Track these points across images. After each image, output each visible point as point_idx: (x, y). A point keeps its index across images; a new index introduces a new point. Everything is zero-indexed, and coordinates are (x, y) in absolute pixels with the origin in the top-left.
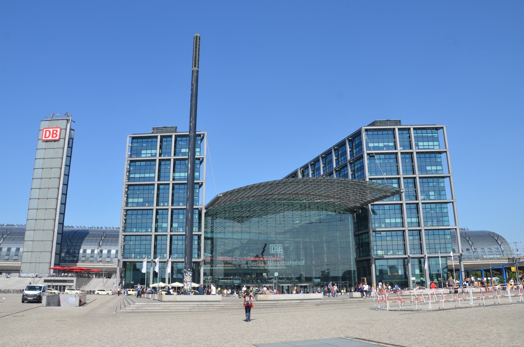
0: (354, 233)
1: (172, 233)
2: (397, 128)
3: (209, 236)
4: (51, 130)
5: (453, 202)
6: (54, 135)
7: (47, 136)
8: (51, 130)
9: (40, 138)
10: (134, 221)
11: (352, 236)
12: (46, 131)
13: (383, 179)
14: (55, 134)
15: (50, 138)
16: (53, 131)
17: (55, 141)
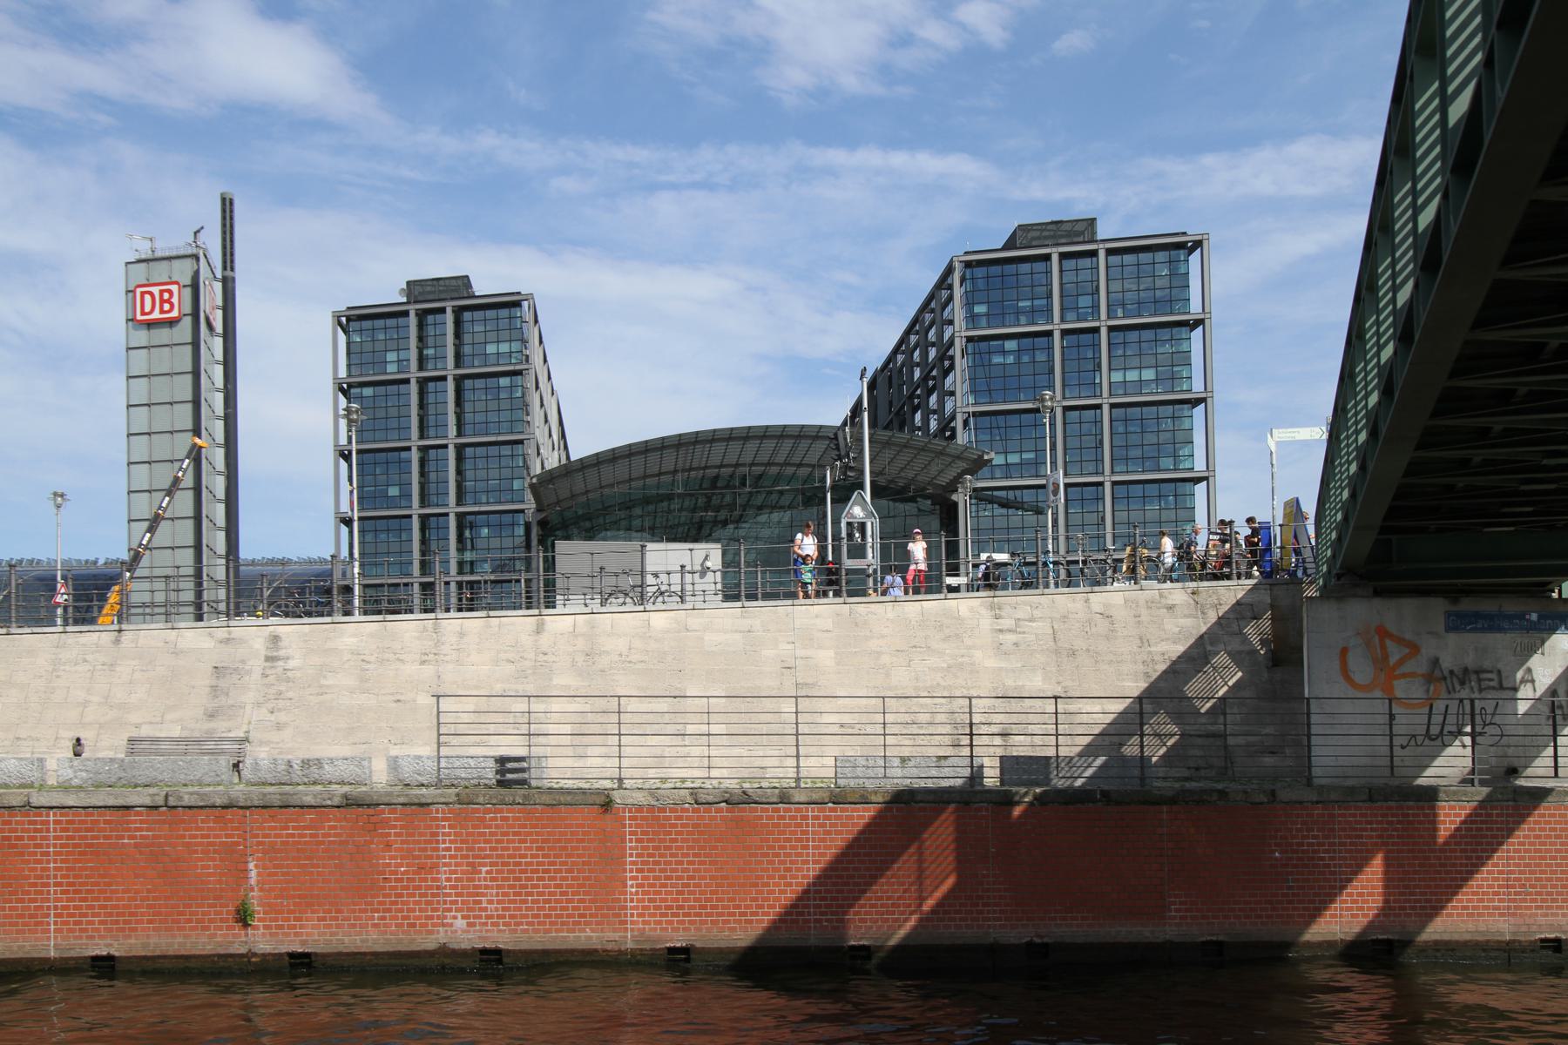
4: (156, 290)
6: (167, 307)
7: (148, 308)
9: (130, 317)
12: (143, 294)
14: (168, 301)
15: (156, 315)
16: (162, 292)
17: (172, 323)
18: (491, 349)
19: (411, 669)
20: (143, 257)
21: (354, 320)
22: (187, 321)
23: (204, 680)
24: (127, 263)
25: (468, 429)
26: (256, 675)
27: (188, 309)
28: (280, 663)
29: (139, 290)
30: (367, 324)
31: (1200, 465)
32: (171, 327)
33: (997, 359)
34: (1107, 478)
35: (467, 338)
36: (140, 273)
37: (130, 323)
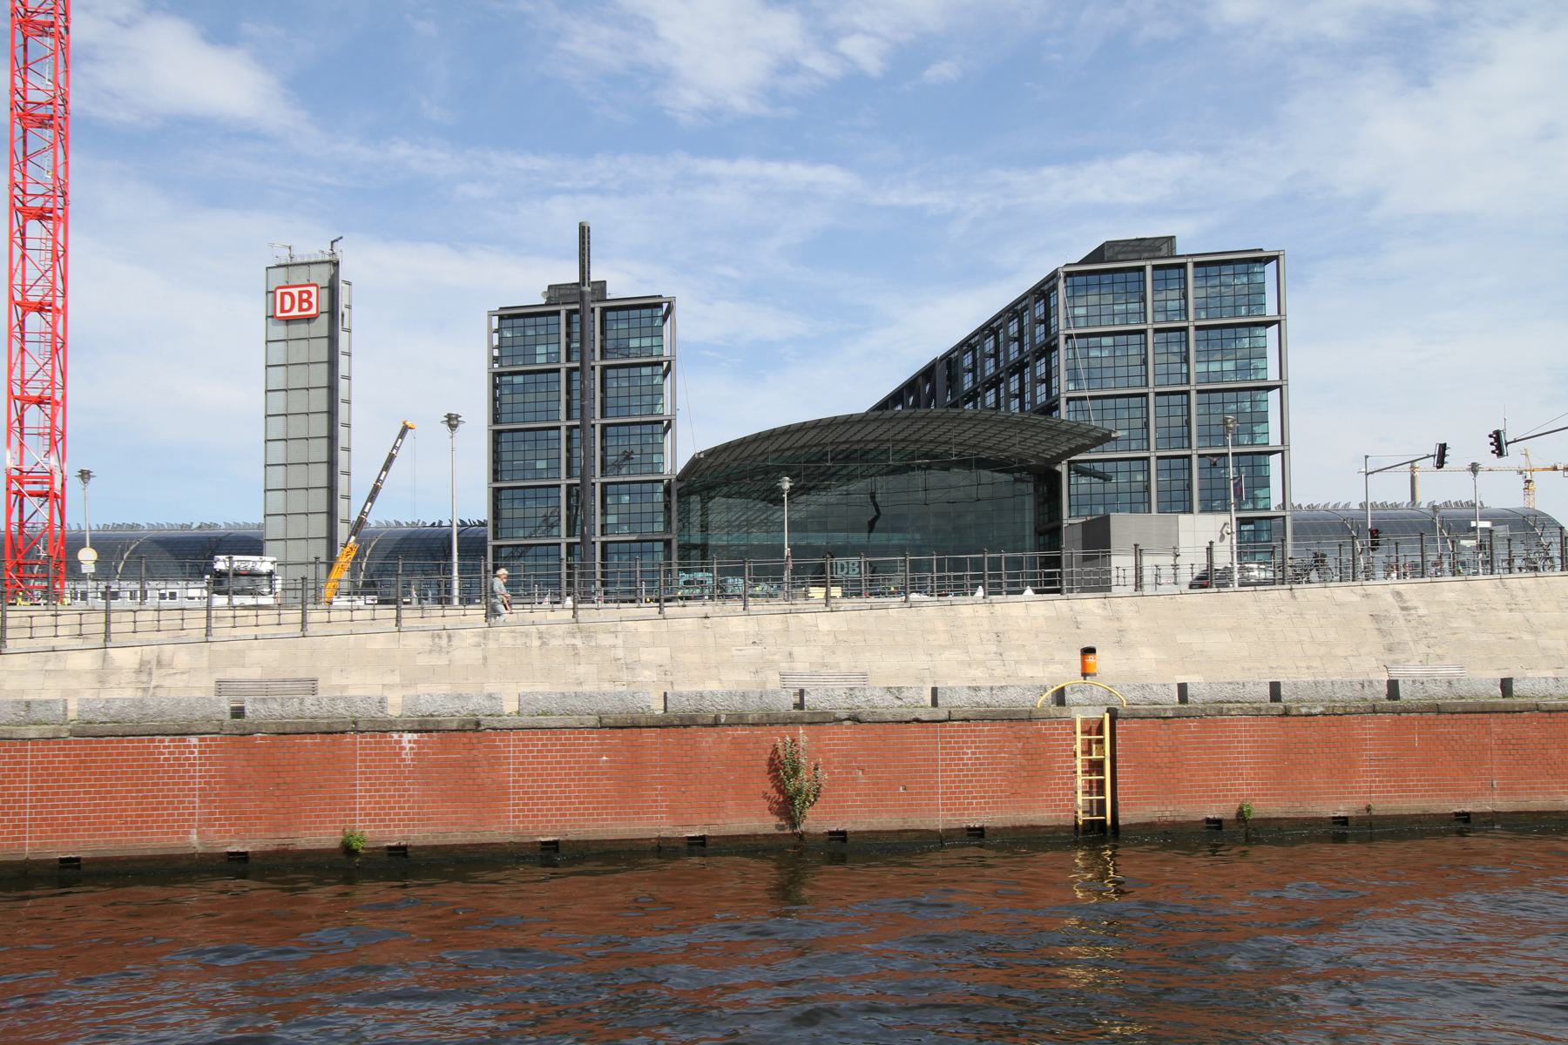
0: (1035, 529)
1: (604, 539)
2: (1148, 265)
3: (696, 538)
4: (295, 291)
5: (1282, 452)
6: (305, 305)
7: (287, 307)
8: (295, 291)
9: (270, 314)
10: (519, 513)
11: (1030, 536)
12: (283, 295)
13: (1084, 398)
14: (307, 300)
15: (295, 312)
16: (301, 293)
17: (309, 319)
18: (634, 343)
19: (1505, 615)
20: (283, 262)
21: (509, 317)
22: (324, 318)
23: (1370, 625)
24: (267, 268)
25: (609, 412)
26: (1402, 621)
27: (325, 306)
28: (1412, 612)
29: (279, 291)
30: (519, 322)
31: (1274, 440)
32: (308, 323)
33: (1094, 353)
34: (1194, 452)
35: (610, 334)
36: (279, 277)
37: (269, 320)
